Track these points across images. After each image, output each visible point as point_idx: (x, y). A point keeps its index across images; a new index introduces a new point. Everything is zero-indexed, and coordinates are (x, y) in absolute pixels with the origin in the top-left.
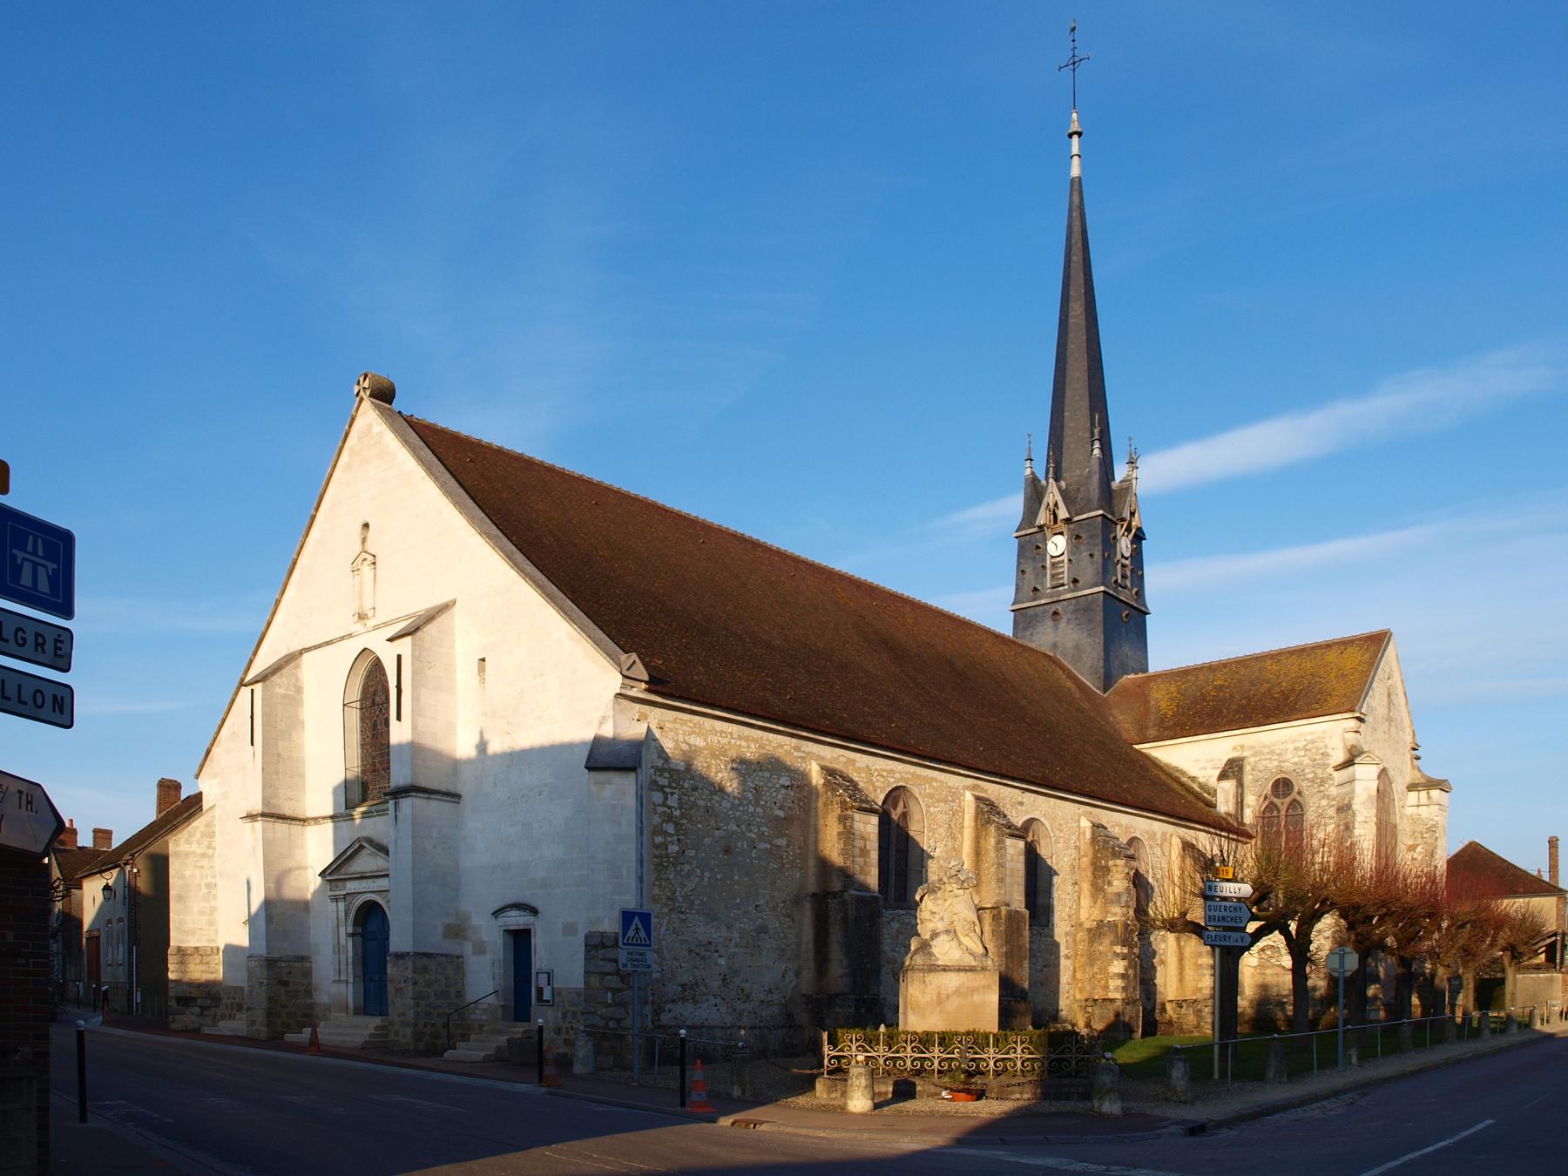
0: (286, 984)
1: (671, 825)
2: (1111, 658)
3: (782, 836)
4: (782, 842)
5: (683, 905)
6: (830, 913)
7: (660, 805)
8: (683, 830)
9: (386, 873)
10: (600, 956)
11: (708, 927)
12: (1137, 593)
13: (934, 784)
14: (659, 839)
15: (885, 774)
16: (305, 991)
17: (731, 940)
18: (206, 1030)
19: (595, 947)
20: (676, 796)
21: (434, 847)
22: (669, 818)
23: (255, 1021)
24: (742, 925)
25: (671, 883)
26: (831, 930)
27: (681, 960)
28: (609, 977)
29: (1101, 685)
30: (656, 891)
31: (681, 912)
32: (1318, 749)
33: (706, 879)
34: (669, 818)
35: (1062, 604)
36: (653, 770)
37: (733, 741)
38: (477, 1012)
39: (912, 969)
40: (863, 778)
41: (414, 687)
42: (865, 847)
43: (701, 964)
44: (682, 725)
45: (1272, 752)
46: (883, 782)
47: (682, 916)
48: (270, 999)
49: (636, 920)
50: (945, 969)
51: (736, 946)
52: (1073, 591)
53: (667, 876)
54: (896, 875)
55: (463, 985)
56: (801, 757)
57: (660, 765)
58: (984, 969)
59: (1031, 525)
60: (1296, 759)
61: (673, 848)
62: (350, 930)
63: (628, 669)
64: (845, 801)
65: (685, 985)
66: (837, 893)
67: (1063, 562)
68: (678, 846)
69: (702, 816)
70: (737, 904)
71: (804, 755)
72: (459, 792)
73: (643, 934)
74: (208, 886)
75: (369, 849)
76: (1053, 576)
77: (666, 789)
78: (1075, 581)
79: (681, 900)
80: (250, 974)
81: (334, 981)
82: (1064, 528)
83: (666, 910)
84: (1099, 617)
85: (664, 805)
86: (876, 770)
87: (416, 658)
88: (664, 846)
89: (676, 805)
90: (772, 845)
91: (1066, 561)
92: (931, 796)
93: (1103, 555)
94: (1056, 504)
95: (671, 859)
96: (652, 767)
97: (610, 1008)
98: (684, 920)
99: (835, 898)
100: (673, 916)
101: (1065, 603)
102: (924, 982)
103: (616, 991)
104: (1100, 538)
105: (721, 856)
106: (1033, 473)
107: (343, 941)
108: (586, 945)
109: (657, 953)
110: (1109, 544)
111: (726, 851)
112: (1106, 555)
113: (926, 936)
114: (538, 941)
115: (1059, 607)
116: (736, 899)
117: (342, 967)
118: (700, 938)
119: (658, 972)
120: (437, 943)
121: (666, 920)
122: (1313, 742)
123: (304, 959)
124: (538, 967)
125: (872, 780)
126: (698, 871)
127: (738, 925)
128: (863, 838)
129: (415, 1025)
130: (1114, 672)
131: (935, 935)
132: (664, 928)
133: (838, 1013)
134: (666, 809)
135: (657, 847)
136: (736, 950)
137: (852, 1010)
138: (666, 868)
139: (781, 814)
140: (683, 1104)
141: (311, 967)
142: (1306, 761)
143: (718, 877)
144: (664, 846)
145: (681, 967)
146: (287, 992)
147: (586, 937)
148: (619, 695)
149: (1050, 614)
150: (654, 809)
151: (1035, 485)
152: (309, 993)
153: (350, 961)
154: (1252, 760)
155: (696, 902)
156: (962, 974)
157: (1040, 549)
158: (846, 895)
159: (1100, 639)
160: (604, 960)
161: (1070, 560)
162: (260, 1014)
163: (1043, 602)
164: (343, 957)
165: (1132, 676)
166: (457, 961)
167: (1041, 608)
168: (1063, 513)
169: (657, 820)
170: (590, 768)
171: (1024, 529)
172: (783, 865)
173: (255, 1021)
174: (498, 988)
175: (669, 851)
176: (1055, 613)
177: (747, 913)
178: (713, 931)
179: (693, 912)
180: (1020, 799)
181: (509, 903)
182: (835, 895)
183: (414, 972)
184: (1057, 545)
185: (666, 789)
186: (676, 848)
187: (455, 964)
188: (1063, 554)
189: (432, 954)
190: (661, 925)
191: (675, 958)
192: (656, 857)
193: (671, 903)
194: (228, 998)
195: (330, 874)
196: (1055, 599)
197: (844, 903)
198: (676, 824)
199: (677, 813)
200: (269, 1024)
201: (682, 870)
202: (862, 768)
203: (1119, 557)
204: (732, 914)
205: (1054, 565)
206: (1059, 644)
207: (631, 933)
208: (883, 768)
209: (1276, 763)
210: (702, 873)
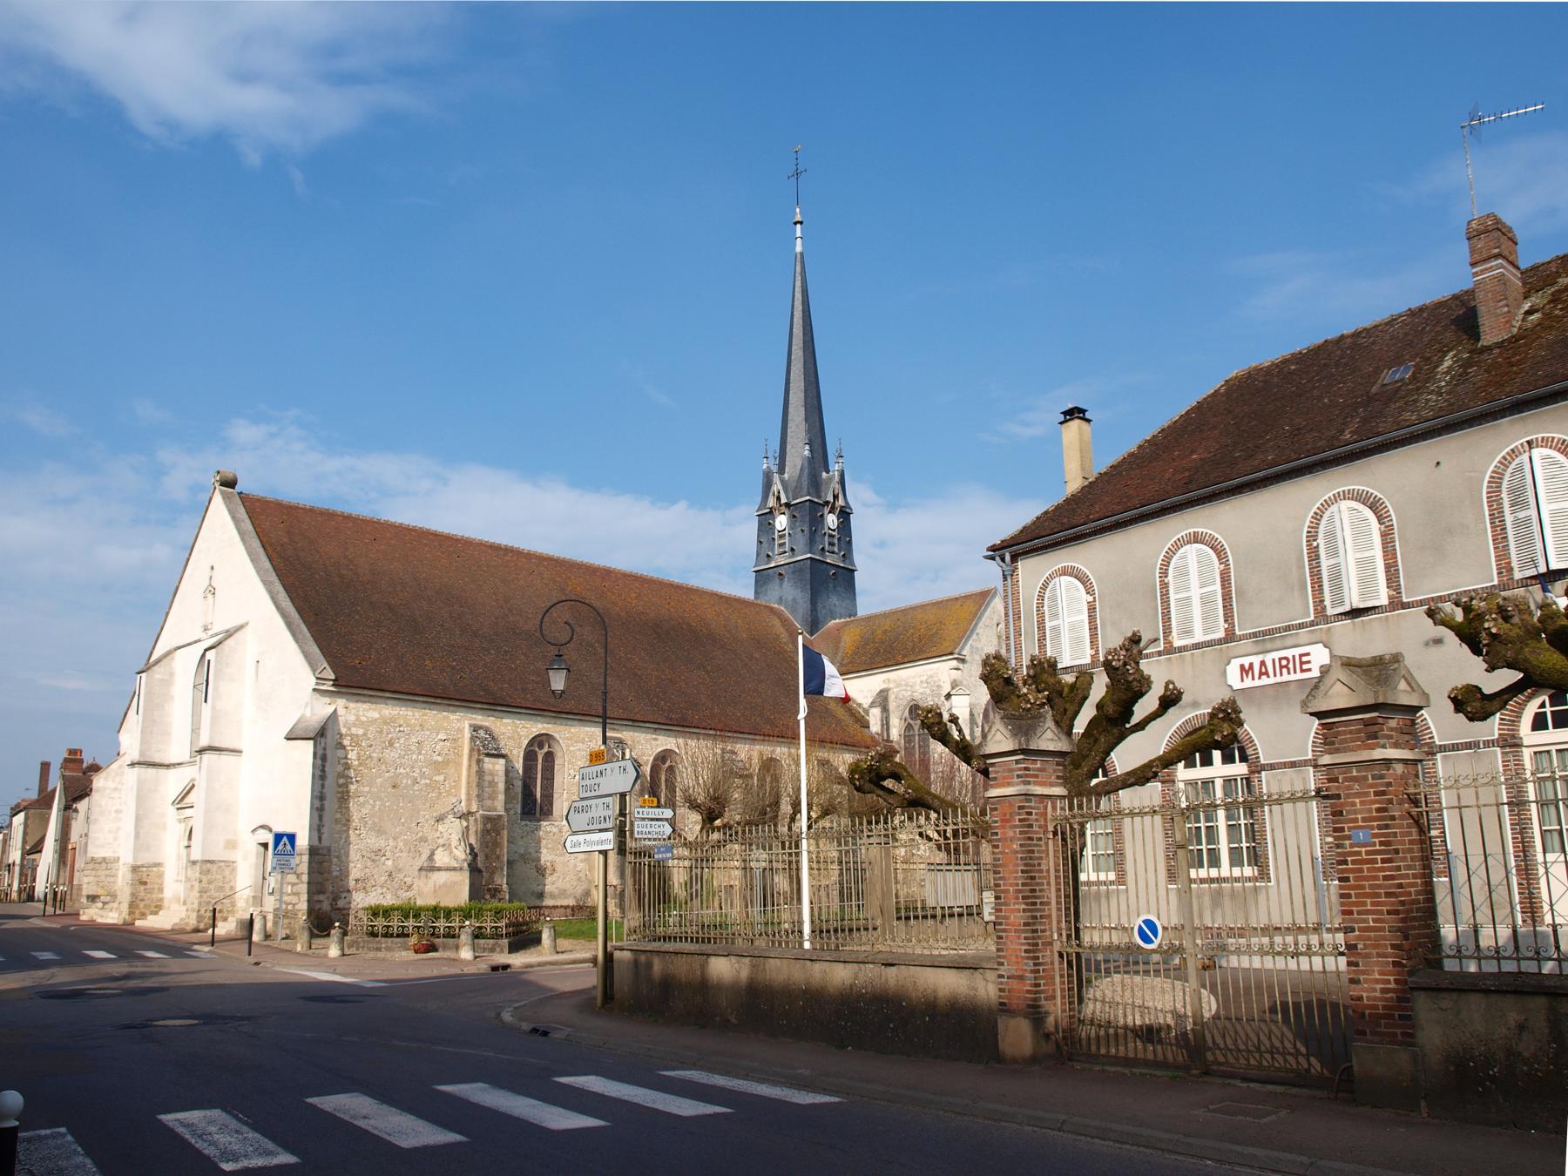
0: (145, 883)
2: (819, 609)
3: (440, 774)
4: (441, 778)
12: (844, 556)
14: (341, 781)
20: (355, 752)
30: (338, 816)
32: (935, 682)
41: (215, 681)
45: (906, 685)
47: (357, 832)
48: (133, 895)
49: (285, 839)
50: (439, 869)
52: (791, 557)
58: (461, 869)
60: (922, 690)
73: (289, 847)
74: (118, 811)
78: (792, 550)
82: (786, 511)
84: (808, 576)
87: (216, 661)
93: (811, 529)
94: (779, 492)
110: (816, 521)
120: (218, 853)
122: (931, 677)
123: (158, 865)
126: (371, 801)
129: (199, 911)
130: (822, 619)
135: (340, 786)
139: (440, 759)
142: (928, 691)
148: (314, 690)
152: (161, 890)
154: (895, 690)
157: (771, 526)
159: (808, 595)
162: (125, 907)
163: (772, 565)
166: (230, 865)
168: (784, 500)
172: (440, 793)
176: (780, 574)
177: (410, 828)
184: (781, 522)
192: (339, 792)
203: (826, 530)
205: (781, 537)
207: (280, 847)
209: (909, 693)
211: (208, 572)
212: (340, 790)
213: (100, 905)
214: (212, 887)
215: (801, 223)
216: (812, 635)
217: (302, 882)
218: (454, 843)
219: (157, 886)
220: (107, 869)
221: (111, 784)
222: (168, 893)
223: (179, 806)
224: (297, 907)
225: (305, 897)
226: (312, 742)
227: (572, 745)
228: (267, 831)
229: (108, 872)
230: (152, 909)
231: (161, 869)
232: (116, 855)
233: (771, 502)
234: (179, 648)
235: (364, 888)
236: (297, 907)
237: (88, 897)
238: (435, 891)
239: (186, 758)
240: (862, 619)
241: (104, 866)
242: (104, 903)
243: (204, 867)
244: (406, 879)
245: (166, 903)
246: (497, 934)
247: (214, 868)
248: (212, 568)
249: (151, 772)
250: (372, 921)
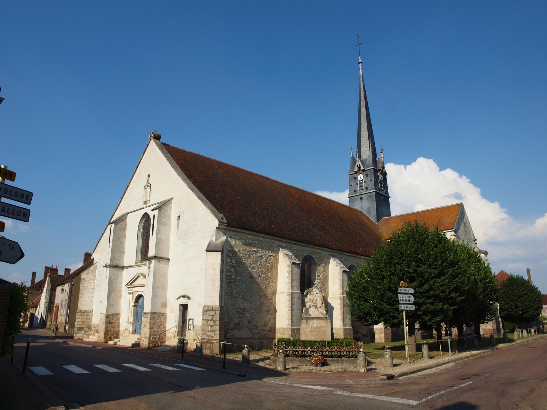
0: (112, 323)
1: (233, 269)
5: (236, 296)
7: (229, 263)
8: (237, 270)
9: (144, 285)
10: (207, 314)
11: (244, 303)
12: (386, 191)
13: (319, 254)
14: (229, 274)
15: (302, 251)
16: (117, 326)
17: (252, 308)
18: (85, 340)
19: (206, 311)
20: (235, 260)
21: (160, 276)
22: (232, 267)
23: (100, 336)
24: (256, 303)
25: (232, 288)
27: (235, 315)
28: (209, 321)
29: (376, 220)
30: (227, 291)
31: (235, 298)
33: (244, 287)
34: (232, 267)
35: (363, 195)
36: (228, 251)
37: (254, 241)
38: (170, 333)
40: (295, 253)
43: (241, 316)
44: (237, 236)
46: (302, 254)
47: (236, 300)
48: (106, 328)
51: (253, 310)
53: (231, 286)
54: (307, 285)
55: (166, 323)
56: (276, 246)
57: (230, 249)
59: (353, 171)
61: (233, 277)
62: (133, 304)
63: (220, 219)
65: (236, 323)
67: (363, 182)
68: (235, 276)
69: (243, 266)
70: (254, 295)
71: (276, 245)
72: (169, 258)
75: (141, 277)
76: (360, 187)
77: (231, 257)
78: (367, 188)
79: (235, 294)
80: (100, 320)
81: (127, 322)
83: (230, 298)
84: (375, 199)
85: (231, 262)
86: (300, 250)
88: (230, 276)
89: (234, 262)
90: (266, 275)
91: (364, 182)
92: (318, 258)
93: (374, 180)
94: (360, 165)
95: (233, 280)
96: (227, 250)
97: (210, 332)
98: (236, 301)
100: (233, 300)
101: (364, 195)
103: (211, 326)
104: (373, 175)
105: (249, 279)
106: (353, 156)
107: (130, 308)
108: (203, 310)
109: (227, 313)
111: (251, 277)
112: (375, 180)
113: (308, 307)
114: (189, 308)
115: (362, 196)
116: (253, 293)
117: (130, 317)
118: (241, 307)
119: (227, 319)
120: (159, 310)
121: (230, 301)
124: (189, 317)
125: (298, 253)
126: (241, 284)
127: (254, 302)
131: (310, 307)
132: (229, 304)
134: (231, 264)
135: (228, 276)
136: (253, 311)
138: (231, 283)
140: (224, 368)
141: (120, 317)
143: (248, 286)
144: (230, 276)
145: (235, 318)
146: (111, 326)
147: (204, 307)
149: (360, 198)
150: (228, 264)
151: (353, 159)
152: (118, 327)
153: (132, 315)
155: (240, 295)
157: (356, 179)
160: (208, 315)
161: (365, 182)
162: (102, 334)
164: (130, 313)
165: (386, 217)
166: (164, 315)
167: (357, 196)
168: (362, 168)
169: (228, 267)
170: (207, 251)
171: (351, 172)
172: (270, 281)
173: (100, 336)
174: (177, 325)
175: (232, 278)
176: (361, 198)
178: (246, 304)
179: (239, 298)
180: (347, 259)
181: (182, 295)
183: (150, 319)
185: (231, 257)
186: (234, 277)
187: (164, 316)
188: (362, 180)
189: (157, 313)
190: (229, 303)
191: (233, 314)
192: (228, 280)
193: (232, 295)
194: (94, 328)
195: (129, 285)
196: (361, 194)
198: (234, 269)
199: (235, 265)
200: (105, 337)
201: (236, 284)
202: (295, 249)
204: (252, 299)
205: (360, 183)
206: (363, 208)
208: (302, 249)
210: (243, 285)
211: (146, 178)
212: (228, 278)
213: (83, 332)
214: (155, 326)
215: (361, 63)
216: (377, 223)
217: (216, 325)
218: (319, 304)
219: (116, 325)
220: (87, 316)
221: (90, 277)
222: (122, 328)
223: (128, 286)
224: (214, 338)
225: (218, 333)
226: (220, 253)
227: (318, 261)
228: (187, 299)
229: (87, 317)
230: (115, 335)
231: (119, 316)
232: (91, 309)
233: (356, 169)
234: (130, 213)
235: (238, 328)
236: (214, 338)
237: (78, 328)
238: (312, 331)
239: (134, 264)
240: (393, 217)
241: (86, 314)
242: (86, 332)
243: (152, 316)
244: (256, 324)
245: (121, 333)
246: (341, 355)
247: (157, 316)
248: (149, 176)
249: (115, 271)
250: (286, 348)
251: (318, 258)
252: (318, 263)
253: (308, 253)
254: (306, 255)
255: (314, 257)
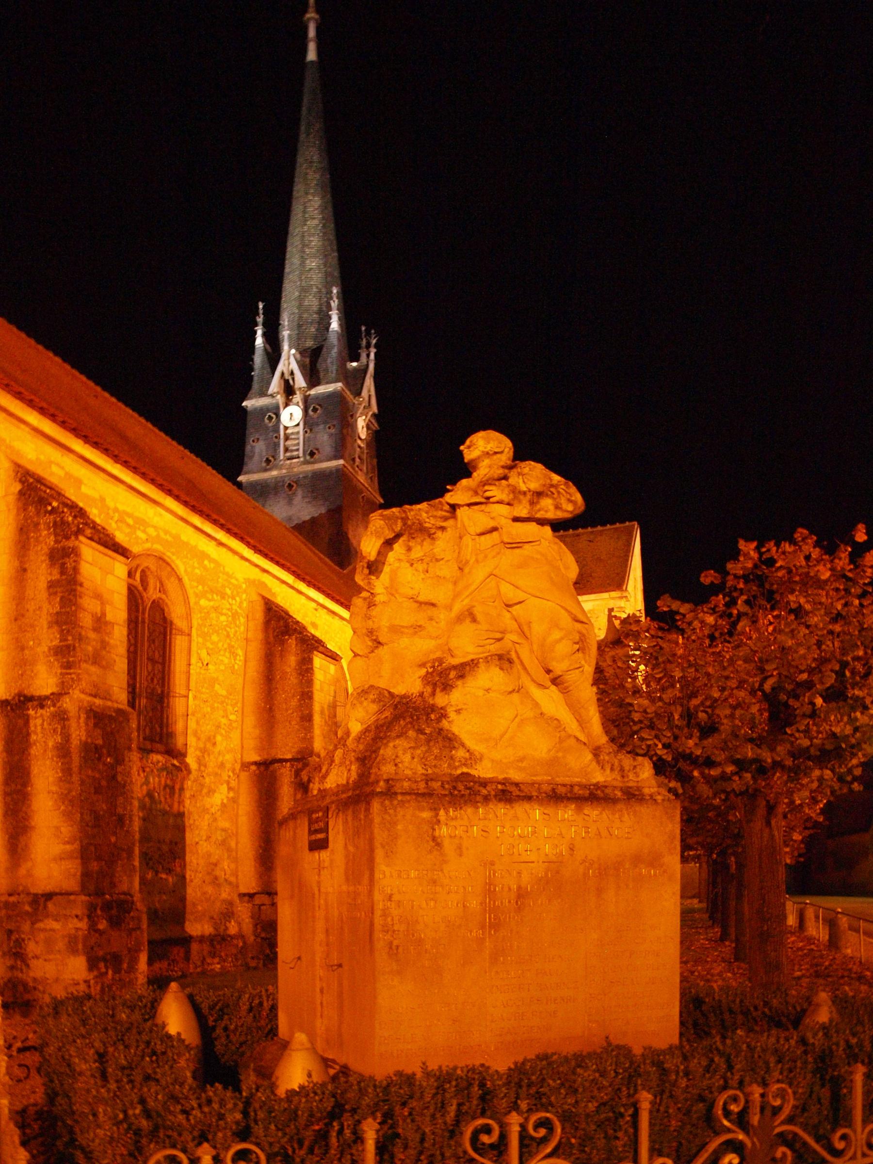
6: (33, 737)
13: (206, 562)
15: (130, 521)
26: (35, 770)
39: (389, 793)
42: (104, 614)
64: (63, 522)
66: (47, 698)
76: (286, 450)
92: (201, 580)
99: (42, 707)
102: (437, 842)
128: (98, 596)
133: (53, 930)
137: (83, 925)
156: (567, 813)
158: (68, 704)
182: (41, 702)
197: (62, 717)
227: (203, 595)
251: (201, 580)
252: (203, 602)
253: (158, 540)
254: (148, 545)
255: (186, 571)
